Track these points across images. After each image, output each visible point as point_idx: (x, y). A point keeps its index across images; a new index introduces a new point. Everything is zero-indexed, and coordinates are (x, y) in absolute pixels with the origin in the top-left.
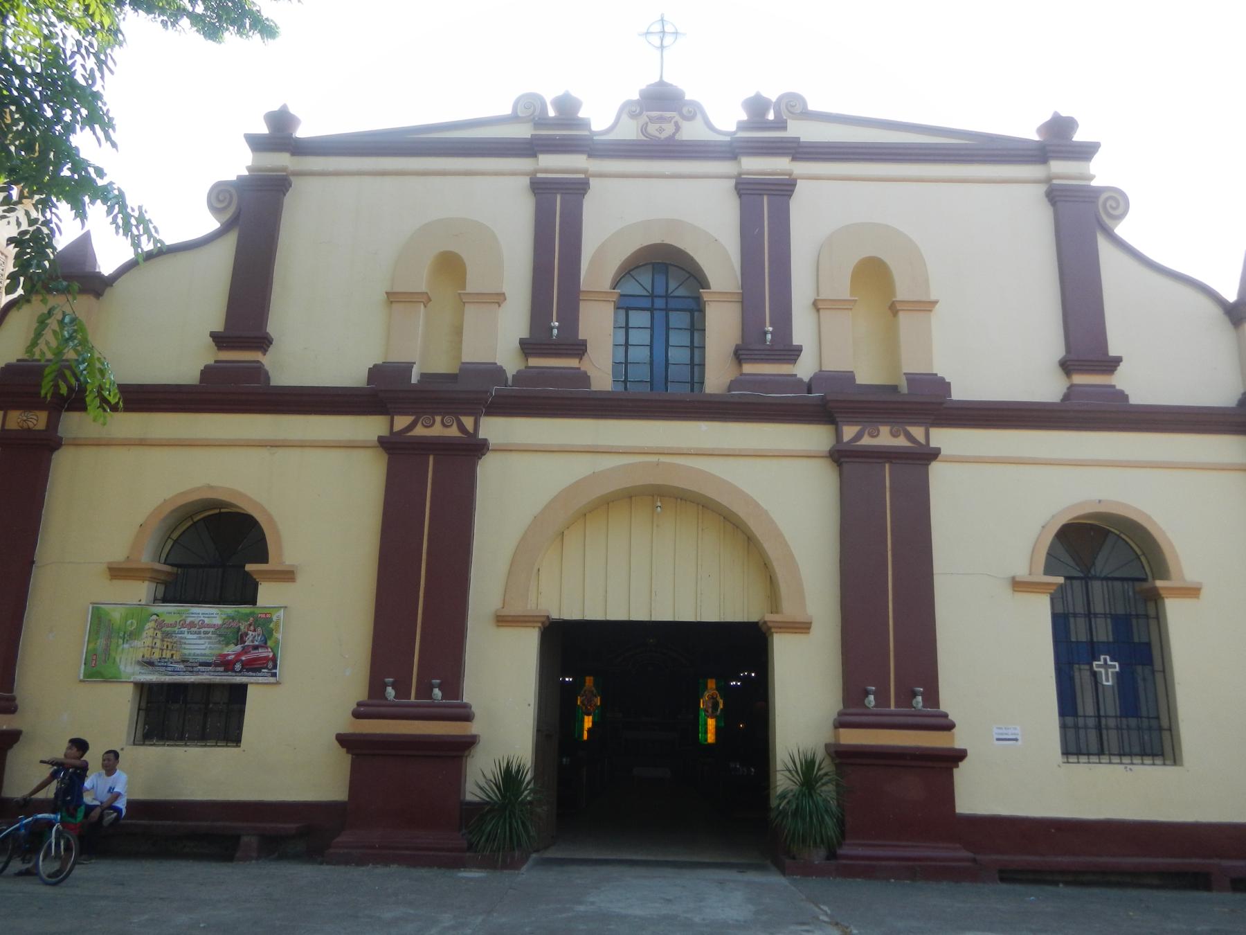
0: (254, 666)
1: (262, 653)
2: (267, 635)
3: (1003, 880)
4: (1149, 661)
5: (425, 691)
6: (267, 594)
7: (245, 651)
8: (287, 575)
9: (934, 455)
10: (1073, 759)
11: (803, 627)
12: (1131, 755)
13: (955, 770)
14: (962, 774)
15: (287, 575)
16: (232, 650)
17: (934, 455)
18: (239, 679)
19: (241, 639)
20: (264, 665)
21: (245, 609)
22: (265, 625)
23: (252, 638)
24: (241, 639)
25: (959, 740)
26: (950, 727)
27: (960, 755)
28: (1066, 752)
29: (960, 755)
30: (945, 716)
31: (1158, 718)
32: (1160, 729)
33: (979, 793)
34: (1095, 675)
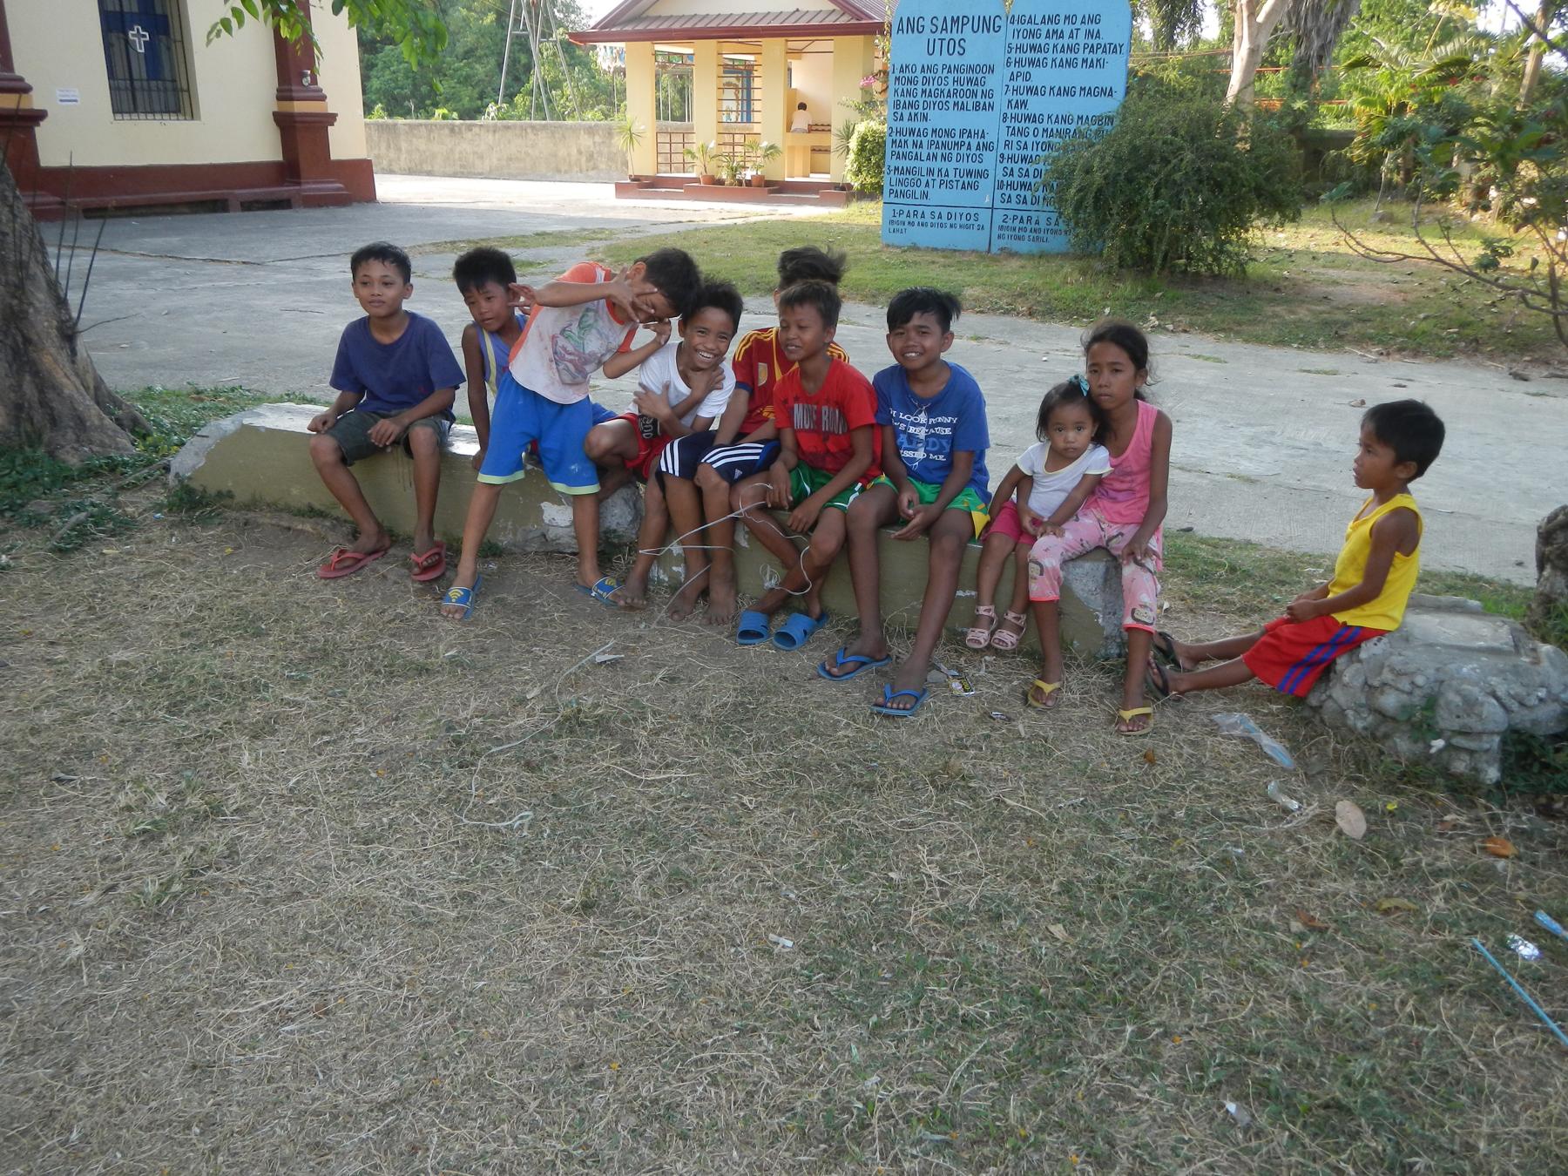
3: (87, 218)
4: (166, 32)
10: (119, 116)
12: (168, 112)
13: (37, 129)
14: (42, 132)
25: (36, 101)
26: (26, 90)
27: (39, 116)
28: (117, 110)
29: (39, 116)
30: (21, 79)
31: (174, 81)
32: (175, 90)
33: (57, 147)
34: (127, 41)
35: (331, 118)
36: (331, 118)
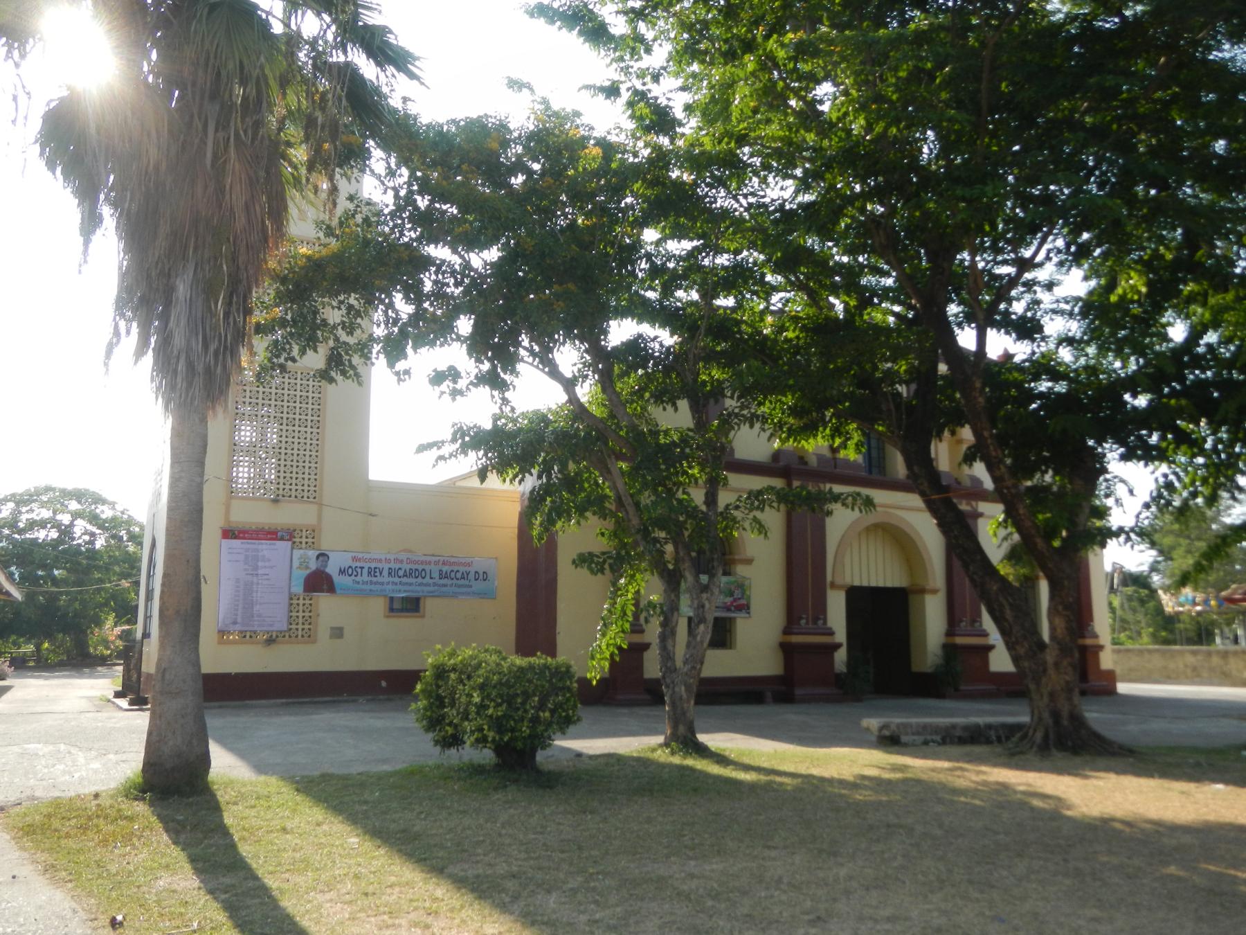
0: (740, 608)
1: (743, 602)
2: (743, 594)
5: (816, 620)
6: (741, 570)
7: (735, 600)
8: (749, 561)
9: (981, 515)
11: (934, 592)
15: (749, 561)
16: (729, 600)
17: (981, 515)
18: (733, 615)
19: (732, 594)
20: (745, 608)
21: (731, 579)
22: (741, 586)
23: (737, 594)
24: (732, 594)
35: (1101, 647)
36: (1101, 647)
